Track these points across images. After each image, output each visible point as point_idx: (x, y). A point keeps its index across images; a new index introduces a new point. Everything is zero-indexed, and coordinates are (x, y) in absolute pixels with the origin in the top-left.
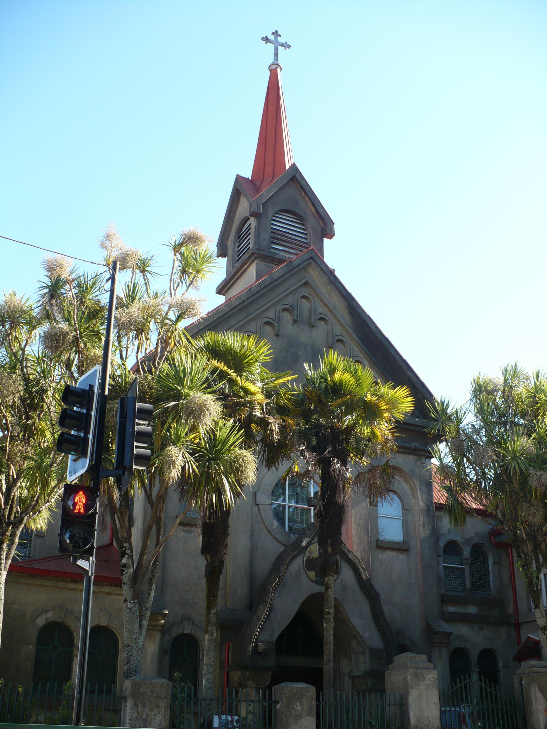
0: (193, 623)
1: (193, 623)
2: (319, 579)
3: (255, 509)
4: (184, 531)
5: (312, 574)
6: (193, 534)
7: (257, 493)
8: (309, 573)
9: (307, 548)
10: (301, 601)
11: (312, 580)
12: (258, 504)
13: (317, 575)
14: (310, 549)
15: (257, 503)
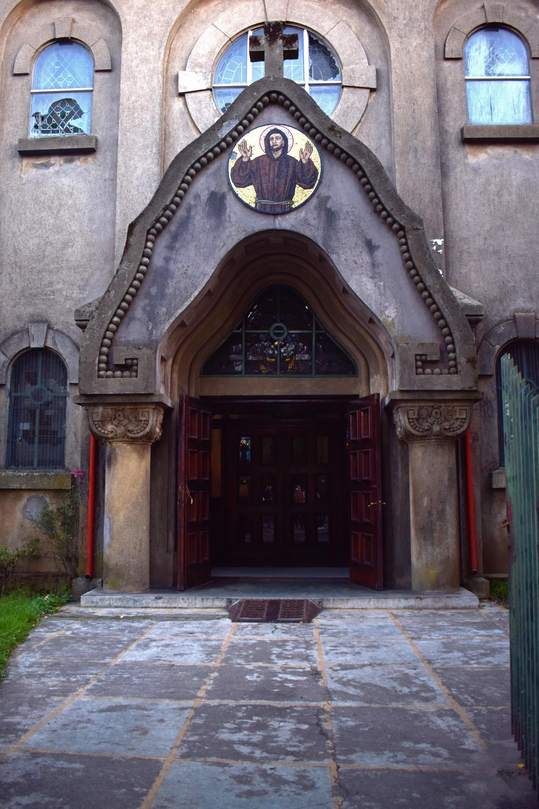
0: (49, 327)
1: (49, 327)
2: (264, 202)
3: (177, 104)
4: (36, 166)
5: (248, 194)
6: (52, 170)
7: (181, 74)
8: (239, 191)
9: (235, 140)
10: (222, 253)
11: (247, 206)
12: (182, 95)
13: (260, 194)
14: (245, 143)
15: (181, 90)
